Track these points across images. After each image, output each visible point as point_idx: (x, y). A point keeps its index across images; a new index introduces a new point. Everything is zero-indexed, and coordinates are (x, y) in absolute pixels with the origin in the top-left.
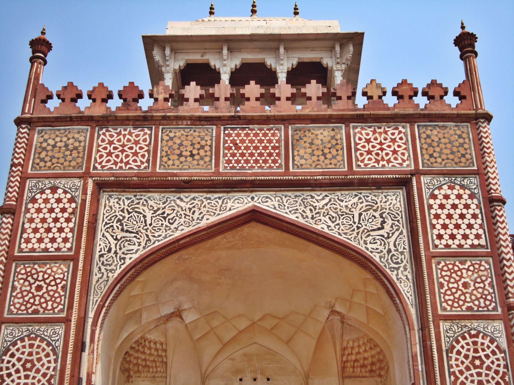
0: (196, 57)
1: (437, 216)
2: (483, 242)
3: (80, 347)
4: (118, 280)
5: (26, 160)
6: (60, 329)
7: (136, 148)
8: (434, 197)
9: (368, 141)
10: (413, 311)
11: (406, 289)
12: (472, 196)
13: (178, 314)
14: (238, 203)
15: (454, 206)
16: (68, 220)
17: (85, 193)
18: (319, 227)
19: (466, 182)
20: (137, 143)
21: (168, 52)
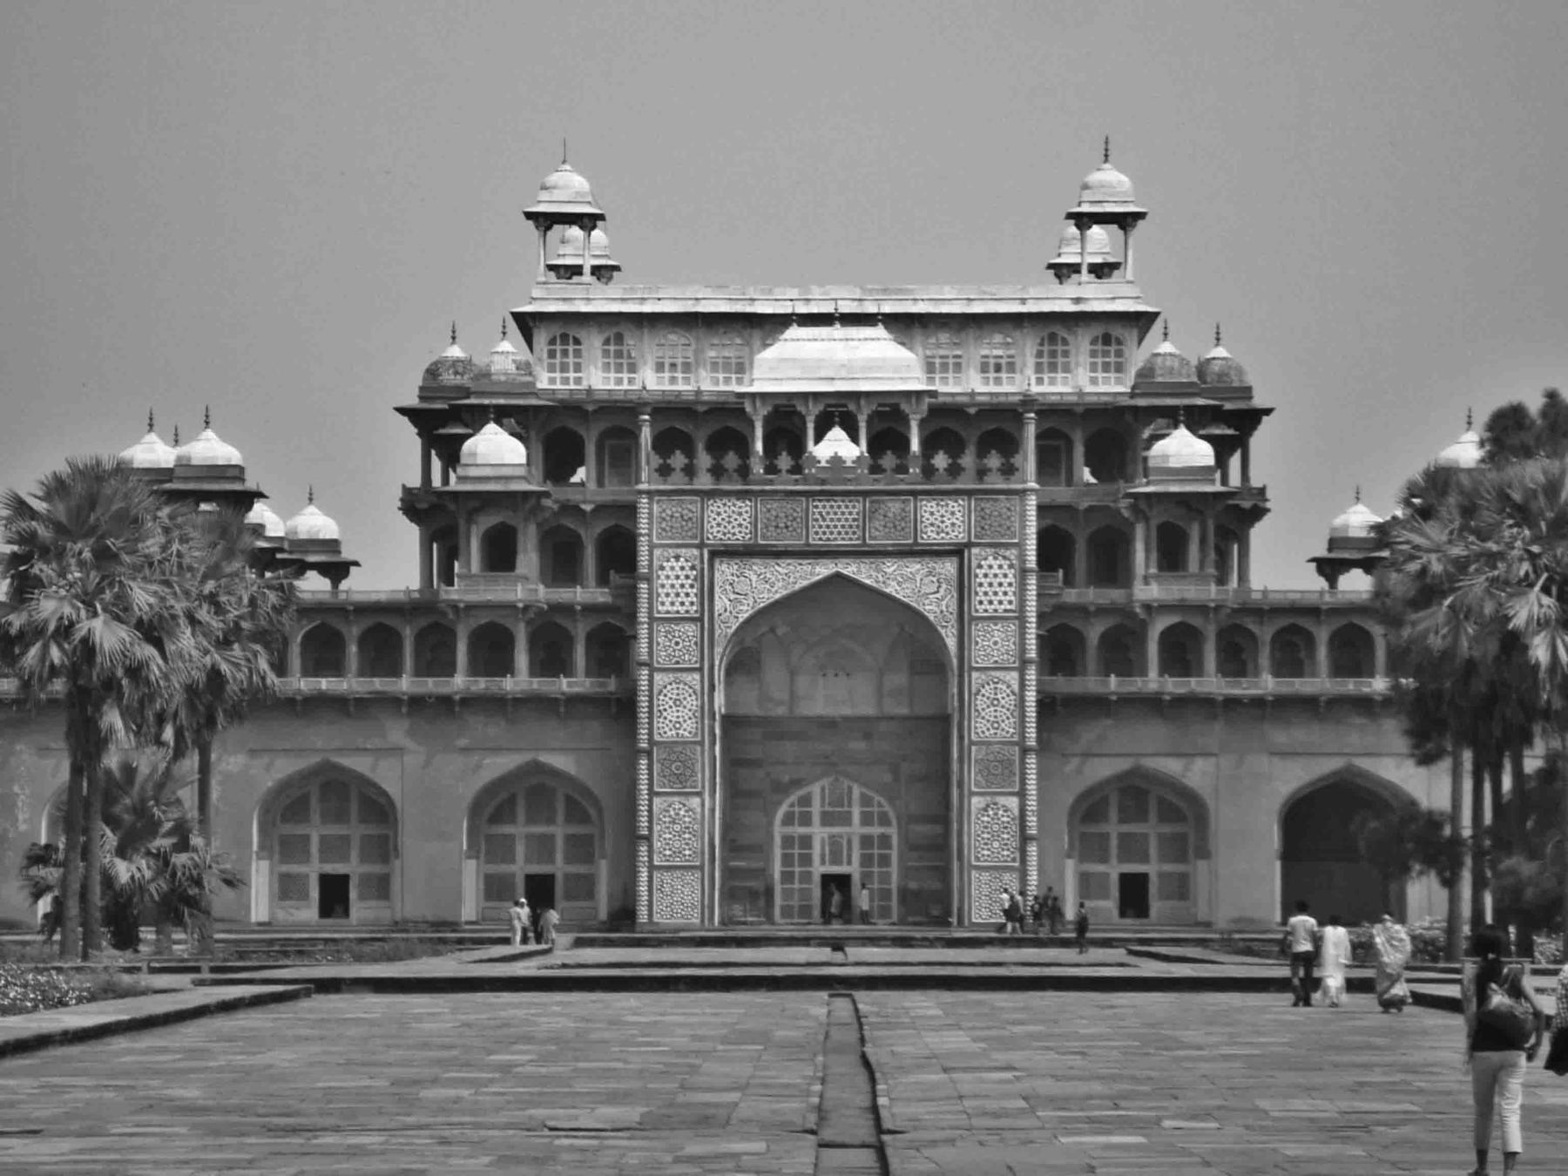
0: (784, 402)
1: (981, 585)
2: (1012, 607)
3: (712, 688)
4: (734, 634)
5: (650, 529)
6: (697, 676)
7: (740, 520)
8: (980, 566)
9: (932, 514)
10: (955, 661)
11: (951, 643)
12: (1011, 566)
13: (772, 630)
14: (823, 569)
15: (996, 576)
16: (692, 586)
17: (702, 562)
18: (888, 590)
19: (1007, 553)
20: (740, 514)
21: (758, 404)
